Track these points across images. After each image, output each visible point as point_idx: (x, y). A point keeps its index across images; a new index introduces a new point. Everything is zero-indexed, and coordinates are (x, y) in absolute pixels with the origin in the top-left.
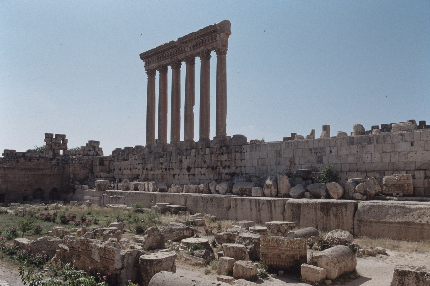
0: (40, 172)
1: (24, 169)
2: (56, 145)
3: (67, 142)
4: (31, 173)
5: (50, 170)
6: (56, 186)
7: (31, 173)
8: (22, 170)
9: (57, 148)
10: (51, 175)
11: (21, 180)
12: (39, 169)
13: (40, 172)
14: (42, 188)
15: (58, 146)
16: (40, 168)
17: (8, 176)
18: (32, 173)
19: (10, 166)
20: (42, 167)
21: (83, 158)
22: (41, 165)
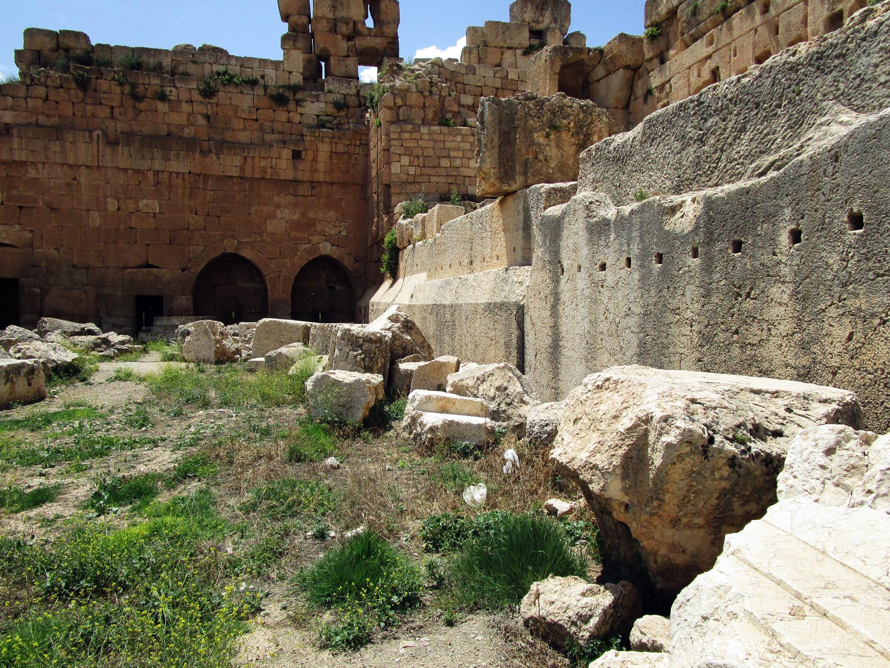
0: (229, 164)
1: (129, 137)
2: (334, 30)
3: (397, 21)
4: (175, 166)
5: (287, 154)
6: (326, 249)
7: (175, 166)
8: (113, 143)
9: (344, 45)
10: (296, 181)
11: (112, 205)
12: (224, 146)
13: (229, 164)
14: (247, 253)
15: (349, 38)
16: (229, 136)
17: (32, 173)
18: (181, 165)
19: (42, 120)
20: (243, 137)
21: (470, 79)
22: (238, 124)
